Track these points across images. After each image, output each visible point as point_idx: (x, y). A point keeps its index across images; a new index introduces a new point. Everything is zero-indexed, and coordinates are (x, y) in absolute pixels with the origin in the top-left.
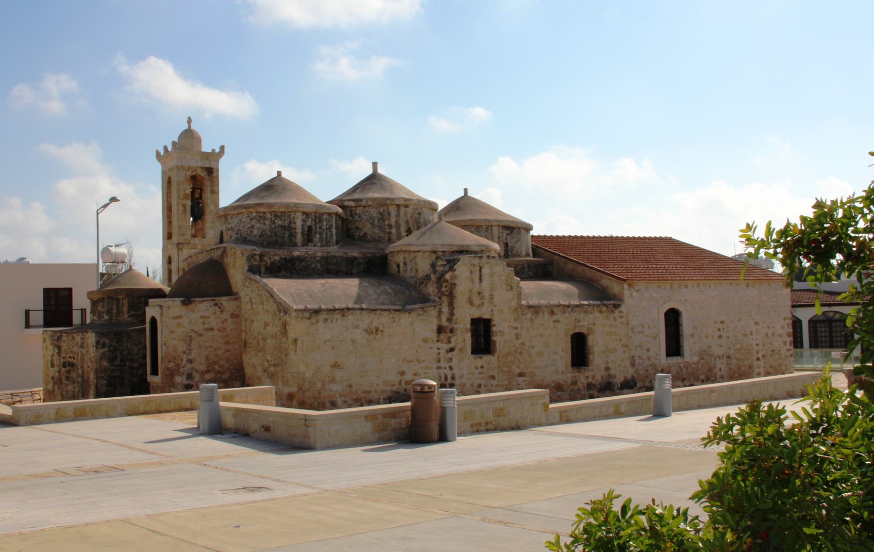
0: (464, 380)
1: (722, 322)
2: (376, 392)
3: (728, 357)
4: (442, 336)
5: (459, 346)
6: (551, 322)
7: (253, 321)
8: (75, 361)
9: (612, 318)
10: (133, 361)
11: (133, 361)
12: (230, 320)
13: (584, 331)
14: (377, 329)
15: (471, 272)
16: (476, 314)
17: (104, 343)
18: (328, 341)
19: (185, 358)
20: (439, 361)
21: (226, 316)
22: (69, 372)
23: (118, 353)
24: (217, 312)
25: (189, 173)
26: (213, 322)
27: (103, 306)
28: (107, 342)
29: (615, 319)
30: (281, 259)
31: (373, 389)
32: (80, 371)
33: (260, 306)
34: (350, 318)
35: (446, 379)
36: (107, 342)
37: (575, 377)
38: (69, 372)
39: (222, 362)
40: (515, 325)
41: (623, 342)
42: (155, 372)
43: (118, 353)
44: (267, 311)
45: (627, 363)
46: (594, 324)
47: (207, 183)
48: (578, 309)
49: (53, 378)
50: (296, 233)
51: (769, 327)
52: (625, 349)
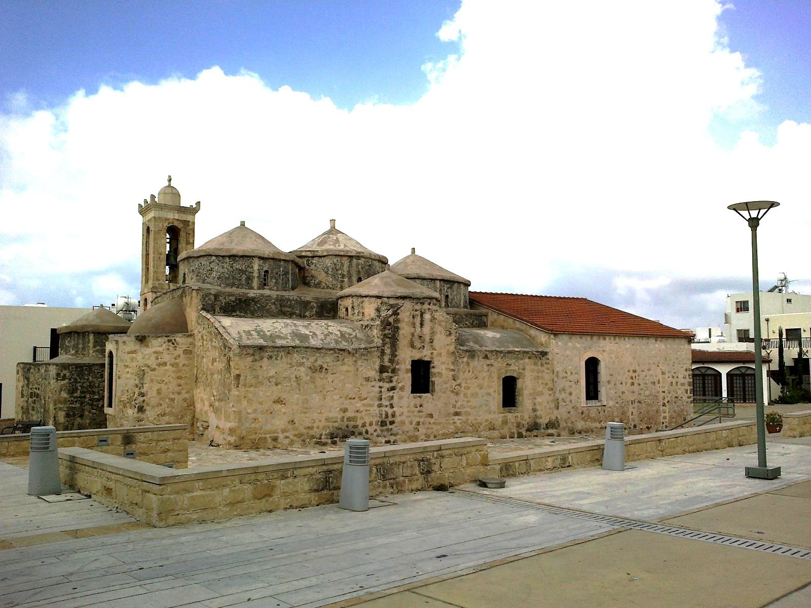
0: (403, 418)
1: (635, 371)
2: (318, 428)
3: (639, 402)
4: (385, 375)
5: (400, 385)
6: (485, 366)
7: (203, 357)
8: (39, 392)
9: (540, 364)
10: (94, 393)
11: (94, 393)
12: (182, 356)
13: (515, 375)
14: (321, 368)
15: (413, 317)
16: (417, 356)
17: (65, 375)
18: (272, 377)
19: (137, 391)
20: (381, 399)
21: (179, 351)
23: (78, 385)
24: (170, 348)
25: (166, 225)
26: (166, 357)
27: (69, 342)
28: (68, 374)
29: (542, 365)
30: (236, 299)
31: (315, 425)
32: (43, 402)
33: (210, 343)
34: (296, 357)
35: (387, 416)
36: (68, 374)
37: (504, 416)
38: (34, 402)
39: (172, 396)
40: (453, 368)
41: (548, 386)
42: (110, 405)
43: (78, 385)
44: (215, 347)
45: (552, 405)
46: (524, 369)
47: (182, 234)
48: (510, 355)
50: (253, 277)
51: (673, 377)
52: (550, 392)
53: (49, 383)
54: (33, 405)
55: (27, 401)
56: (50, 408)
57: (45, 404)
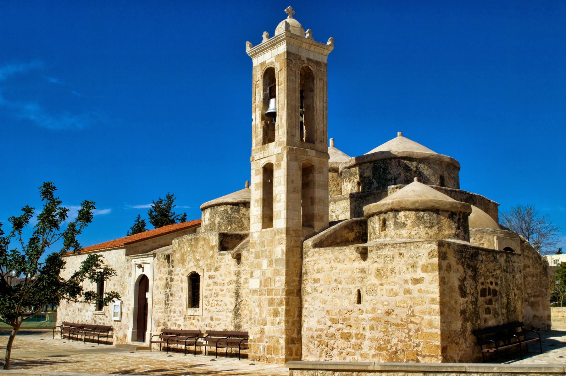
8: (497, 288)
22: (490, 302)
32: (505, 300)
44: (528, 257)
49: (463, 312)
53: (514, 277)
55: (475, 303)
56: (517, 306)
57: (508, 303)
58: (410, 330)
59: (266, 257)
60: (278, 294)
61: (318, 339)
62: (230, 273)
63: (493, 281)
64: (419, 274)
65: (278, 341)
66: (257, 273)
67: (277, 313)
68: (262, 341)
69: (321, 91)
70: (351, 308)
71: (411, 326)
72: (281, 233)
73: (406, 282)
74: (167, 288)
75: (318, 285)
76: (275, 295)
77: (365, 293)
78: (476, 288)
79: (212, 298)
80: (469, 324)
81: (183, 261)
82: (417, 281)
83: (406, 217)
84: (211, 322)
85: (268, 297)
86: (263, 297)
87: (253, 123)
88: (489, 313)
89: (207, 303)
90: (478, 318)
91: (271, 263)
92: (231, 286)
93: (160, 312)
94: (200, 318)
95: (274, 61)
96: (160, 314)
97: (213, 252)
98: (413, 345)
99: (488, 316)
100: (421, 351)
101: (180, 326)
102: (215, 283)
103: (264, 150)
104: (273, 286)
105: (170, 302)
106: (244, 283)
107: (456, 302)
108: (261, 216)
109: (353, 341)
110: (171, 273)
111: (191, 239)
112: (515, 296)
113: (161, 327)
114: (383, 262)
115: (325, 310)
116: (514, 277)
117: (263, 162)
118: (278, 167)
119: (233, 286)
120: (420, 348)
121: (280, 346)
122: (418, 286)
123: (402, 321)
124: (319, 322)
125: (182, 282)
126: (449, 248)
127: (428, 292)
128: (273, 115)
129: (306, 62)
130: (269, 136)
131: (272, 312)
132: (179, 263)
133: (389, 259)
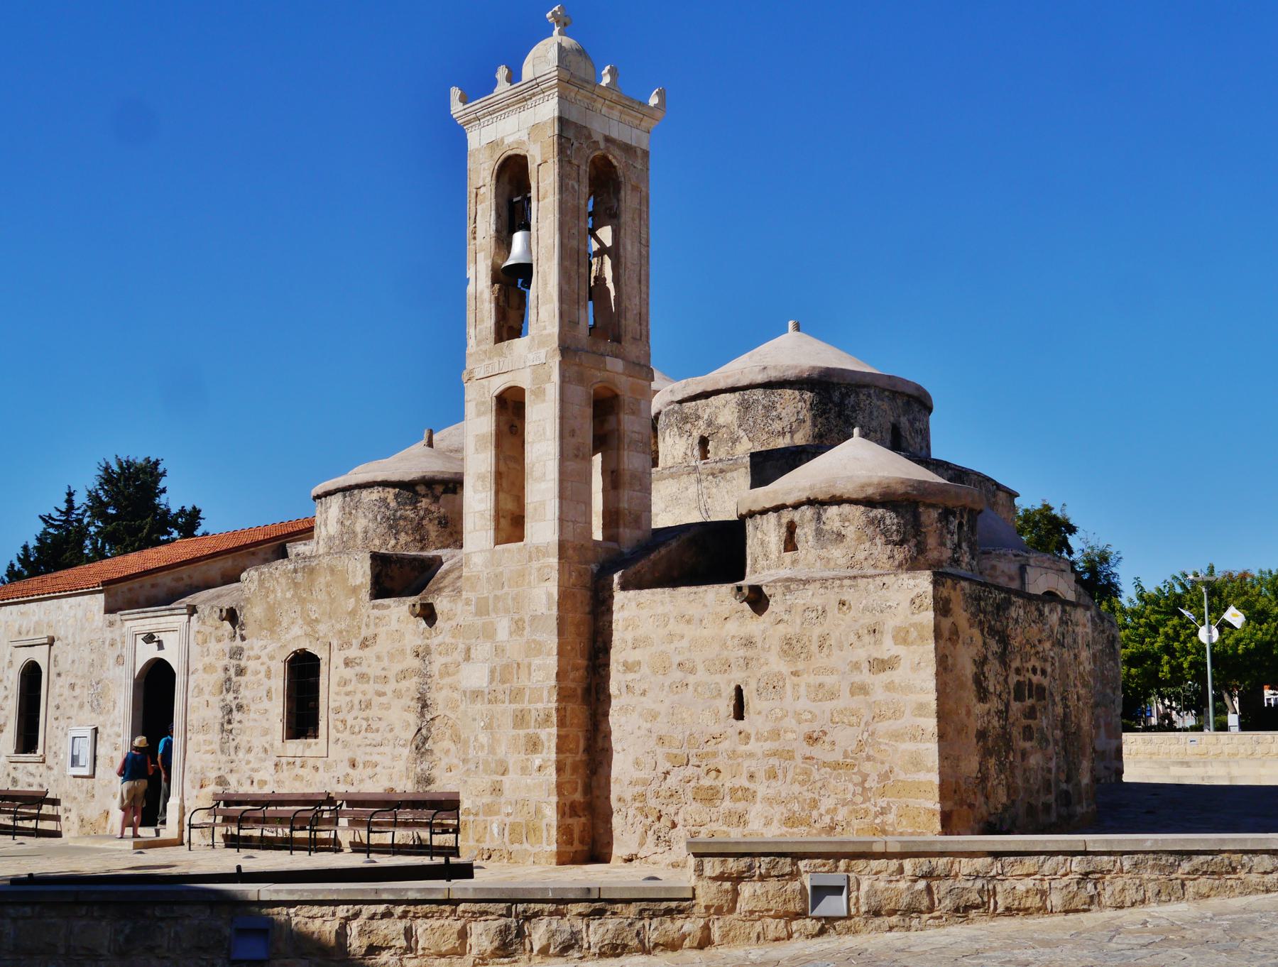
8: (1045, 682)
22: (1031, 713)
32: (1059, 710)
38: (1031, 713)
49: (982, 735)
53: (1076, 656)
54: (1025, 722)
58: (865, 778)
59: (507, 611)
60: (540, 699)
61: (637, 804)
62: (403, 651)
63: (1038, 665)
64: (888, 648)
65: (538, 811)
66: (482, 650)
67: (535, 744)
68: (497, 813)
69: (636, 216)
70: (716, 729)
71: (867, 767)
72: (546, 554)
73: (856, 666)
74: (228, 691)
75: (637, 676)
76: (530, 702)
77: (755, 693)
78: (1006, 680)
79: (355, 712)
80: (992, 762)
81: (272, 624)
82: (881, 665)
83: (844, 519)
84: (350, 771)
85: (514, 706)
86: (499, 708)
87: (470, 289)
88: (1031, 739)
89: (340, 725)
90: (1009, 747)
91: (518, 626)
92: (404, 684)
93: (207, 752)
94: (319, 763)
95: (526, 138)
96: (208, 756)
97: (357, 602)
98: (874, 809)
99: (1028, 745)
100: (892, 825)
101: (263, 783)
102: (362, 677)
103: (501, 355)
104: (524, 682)
105: (235, 725)
106: (441, 676)
107: (968, 713)
108: (493, 512)
109: (727, 804)
110: (237, 653)
111: (295, 571)
112: (1078, 700)
113: (212, 788)
114: (798, 622)
115: (654, 736)
116: (1076, 656)
117: (498, 385)
118: (537, 396)
119: (412, 684)
120: (891, 818)
121: (544, 822)
122: (885, 677)
123: (846, 755)
124: (637, 763)
125: (268, 676)
126: (955, 590)
127: (908, 689)
128: (524, 272)
129: (602, 145)
130: (510, 323)
131: (522, 741)
132: (261, 628)
133: (814, 614)
